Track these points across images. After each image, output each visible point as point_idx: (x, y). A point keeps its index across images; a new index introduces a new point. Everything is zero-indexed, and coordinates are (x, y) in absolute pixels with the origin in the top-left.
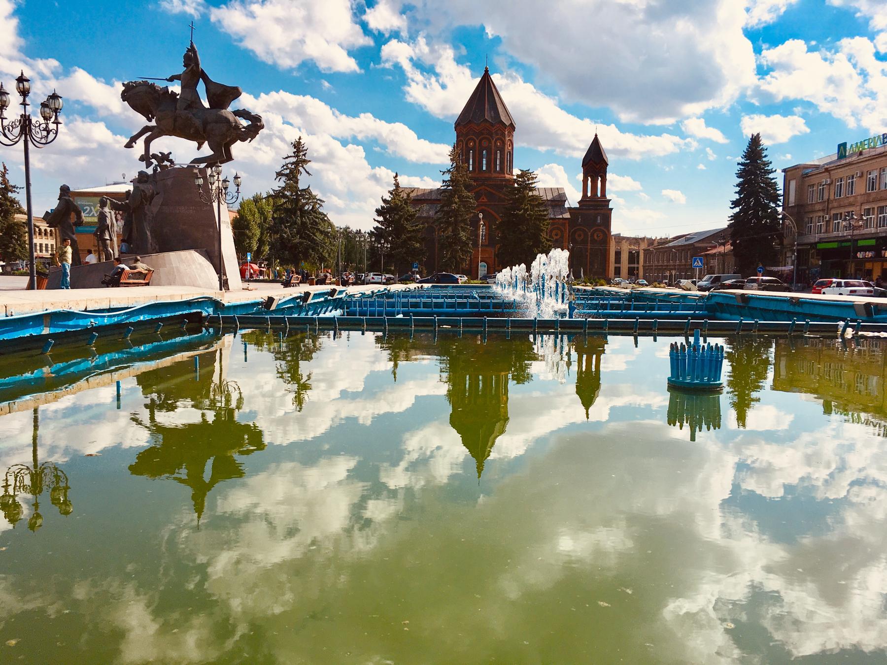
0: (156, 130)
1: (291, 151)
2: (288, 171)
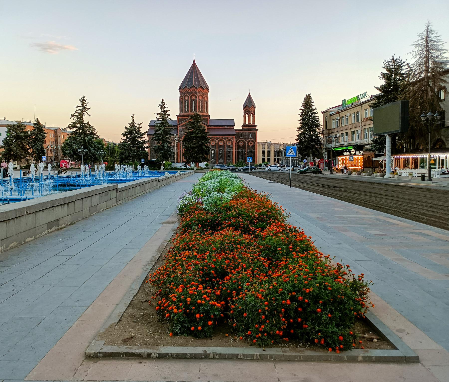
1: (79, 104)
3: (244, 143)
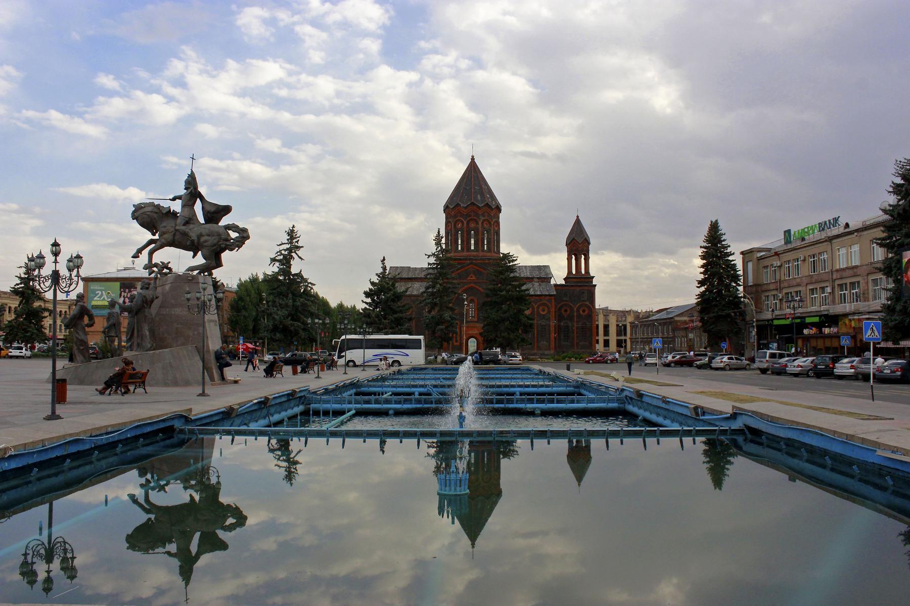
0: (158, 243)
1: (285, 238)
2: (281, 257)
3: (572, 310)
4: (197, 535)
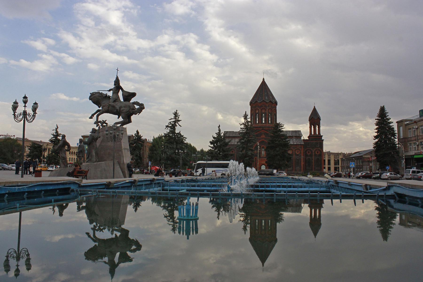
0: (101, 111)
1: (173, 116)
2: (171, 125)
3: (312, 152)
4: (118, 254)
